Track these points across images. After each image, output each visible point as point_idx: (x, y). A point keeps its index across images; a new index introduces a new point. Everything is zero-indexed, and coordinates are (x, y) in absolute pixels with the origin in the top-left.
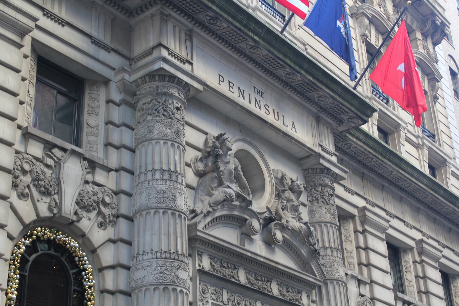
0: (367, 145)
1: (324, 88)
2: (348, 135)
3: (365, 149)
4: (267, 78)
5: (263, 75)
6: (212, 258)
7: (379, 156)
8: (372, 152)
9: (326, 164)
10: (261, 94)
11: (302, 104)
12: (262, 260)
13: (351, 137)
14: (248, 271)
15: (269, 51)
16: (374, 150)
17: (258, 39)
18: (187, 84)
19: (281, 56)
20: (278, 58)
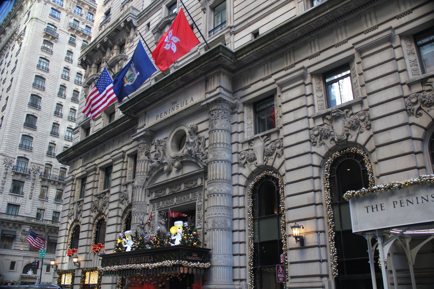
0: (255, 48)
1: (187, 73)
2: (238, 59)
3: (256, 51)
4: (176, 93)
5: (174, 94)
6: (156, 192)
7: (269, 42)
8: (263, 46)
9: (205, 103)
10: (175, 103)
11: (196, 83)
12: (171, 180)
13: (241, 58)
14: (170, 188)
15: (160, 91)
16: (263, 44)
17: (153, 93)
18: (141, 136)
19: (164, 87)
20: (164, 88)
